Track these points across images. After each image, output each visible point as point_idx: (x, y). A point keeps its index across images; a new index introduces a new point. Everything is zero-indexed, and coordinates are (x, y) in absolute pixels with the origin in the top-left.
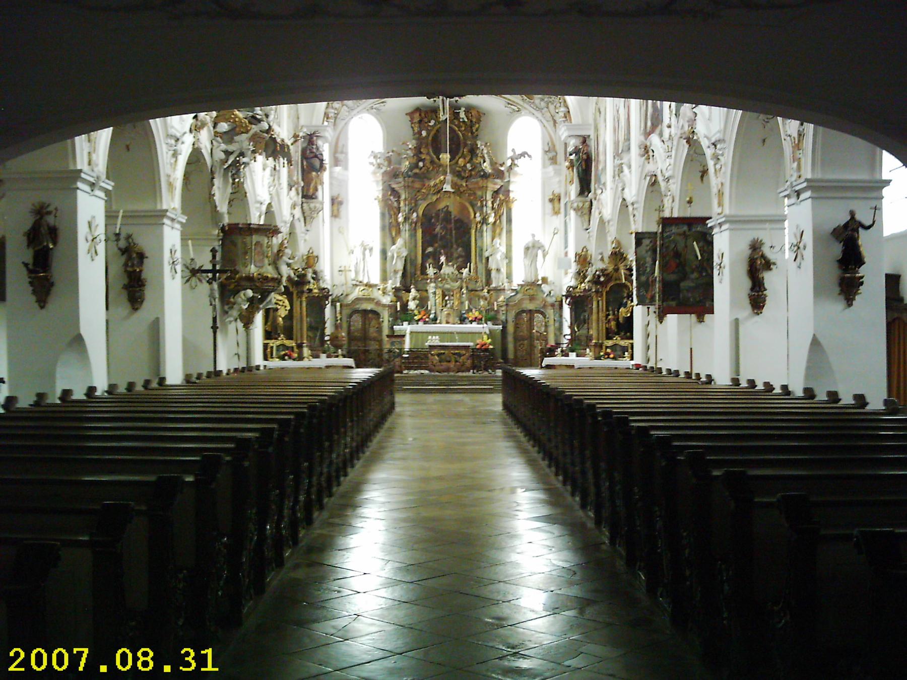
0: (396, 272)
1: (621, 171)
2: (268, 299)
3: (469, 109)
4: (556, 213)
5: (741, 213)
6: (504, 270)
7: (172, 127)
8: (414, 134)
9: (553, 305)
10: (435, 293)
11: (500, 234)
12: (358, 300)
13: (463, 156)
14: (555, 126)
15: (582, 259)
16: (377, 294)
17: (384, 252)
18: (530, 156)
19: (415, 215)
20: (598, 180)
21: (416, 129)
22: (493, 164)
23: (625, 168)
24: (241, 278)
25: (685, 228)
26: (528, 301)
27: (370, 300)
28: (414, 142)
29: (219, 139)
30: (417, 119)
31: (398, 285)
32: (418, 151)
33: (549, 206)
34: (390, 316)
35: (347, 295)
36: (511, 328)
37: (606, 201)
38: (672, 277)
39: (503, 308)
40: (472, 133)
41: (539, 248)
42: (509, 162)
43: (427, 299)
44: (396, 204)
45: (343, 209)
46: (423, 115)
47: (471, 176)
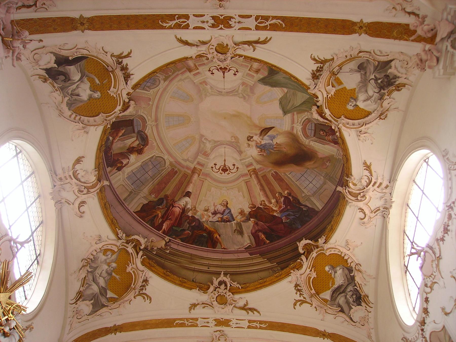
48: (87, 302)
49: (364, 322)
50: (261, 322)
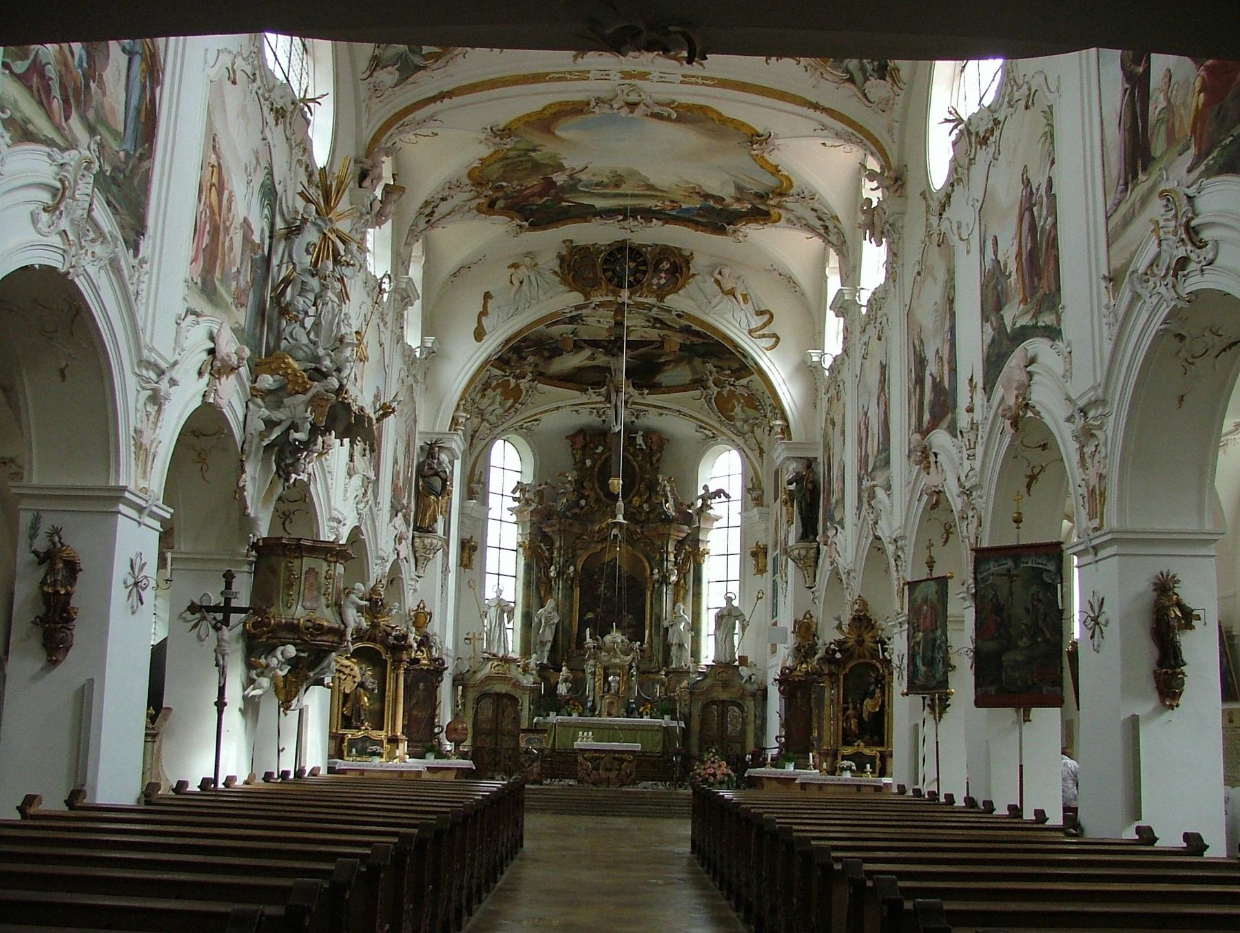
0: (543, 644)
1: (872, 496)
2: (325, 663)
3: (649, 433)
4: (761, 571)
5: (1129, 525)
6: (688, 646)
7: (152, 349)
8: (576, 463)
9: (753, 695)
10: (594, 674)
11: (684, 599)
12: (489, 678)
14: (761, 456)
15: (803, 629)
16: (516, 672)
17: (527, 618)
19: (572, 568)
20: (829, 517)
22: (678, 505)
23: (880, 493)
24: (279, 625)
25: (1010, 563)
27: (505, 679)
28: (575, 473)
29: (259, 401)
30: (578, 446)
31: (545, 661)
32: (579, 485)
33: (752, 561)
36: (695, 725)
37: (845, 544)
38: (991, 646)
40: (652, 464)
41: (737, 617)
42: (700, 503)
43: (584, 680)
44: (547, 554)
45: (476, 557)
47: (648, 519)
48: (390, 68)
49: (885, 106)
50: (704, 78)
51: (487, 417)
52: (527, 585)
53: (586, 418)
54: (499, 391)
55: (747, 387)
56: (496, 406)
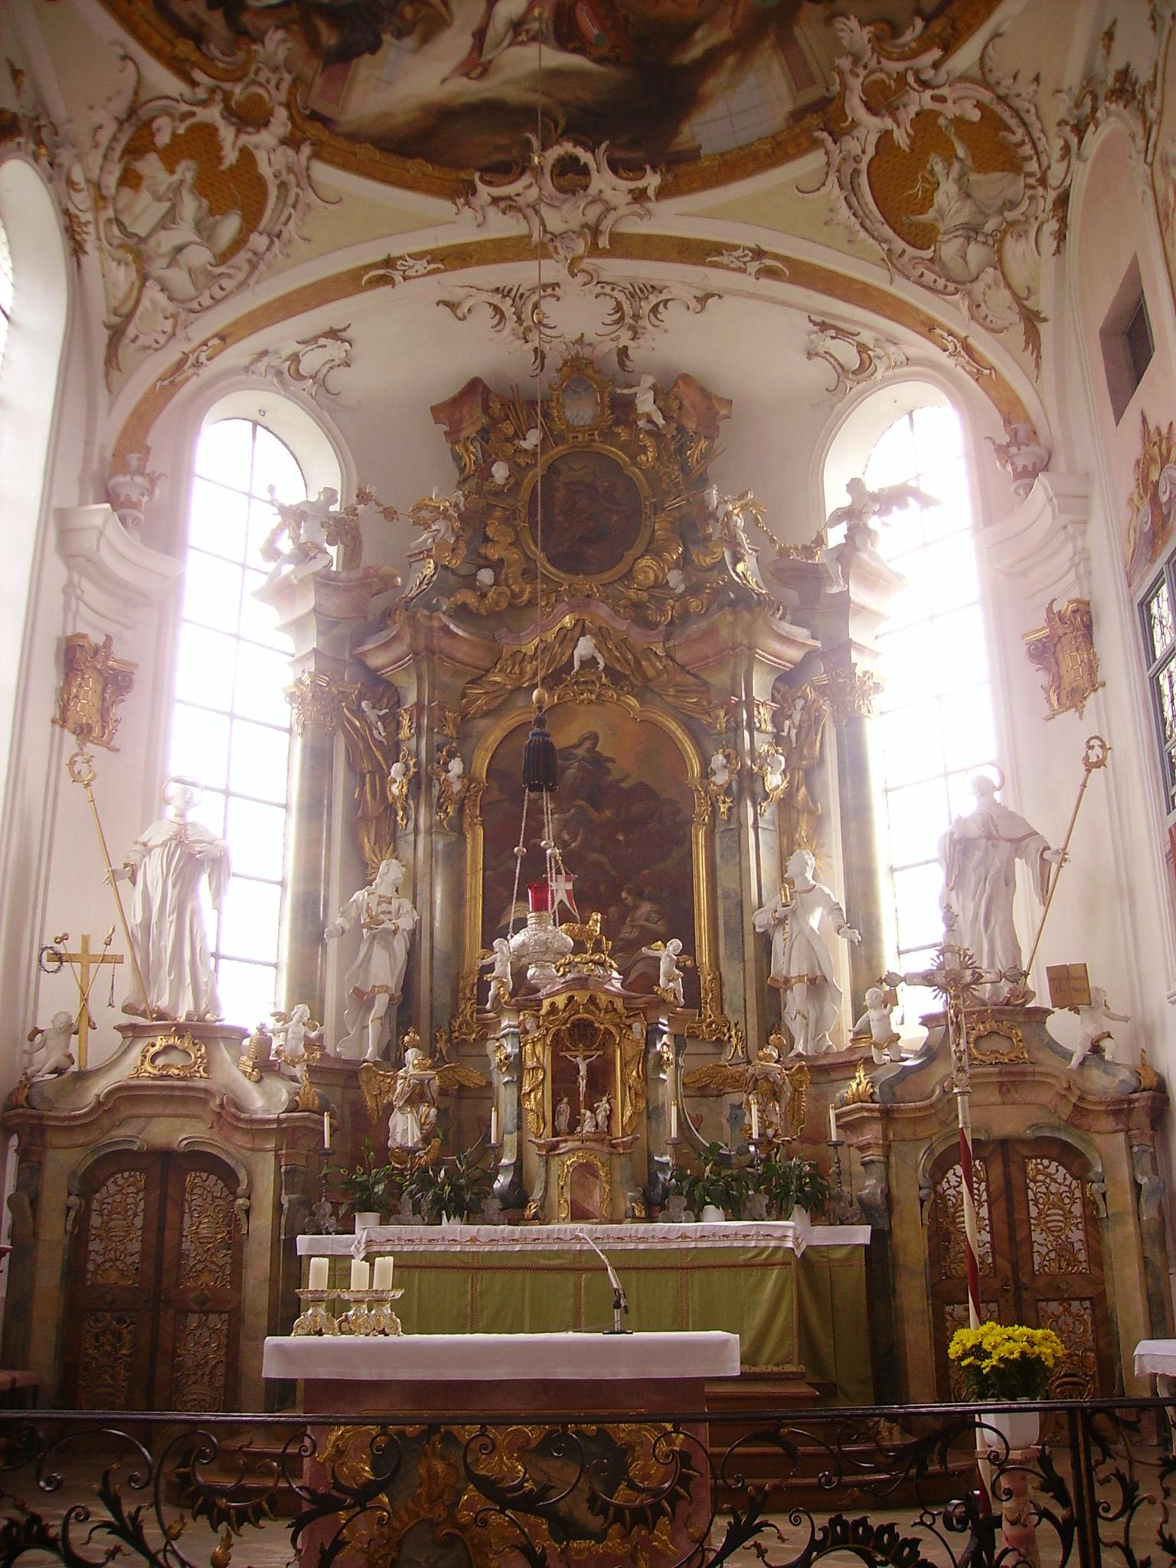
3: (674, 388)
6: (843, 980)
9: (1120, 1109)
10: (516, 1065)
12: (127, 1096)
13: (654, 549)
14: (1032, 337)
16: (232, 1072)
18: (925, 501)
19: (456, 766)
21: (469, 460)
26: (995, 1097)
27: (181, 1096)
30: (469, 430)
34: (287, 1179)
35: (83, 1076)
36: (912, 1241)
39: (871, 1134)
40: (684, 468)
44: (380, 732)
45: (129, 711)
46: (495, 407)
51: (158, 267)
52: (314, 807)
53: (486, 350)
54: (186, 170)
55: (983, 75)
56: (184, 232)
